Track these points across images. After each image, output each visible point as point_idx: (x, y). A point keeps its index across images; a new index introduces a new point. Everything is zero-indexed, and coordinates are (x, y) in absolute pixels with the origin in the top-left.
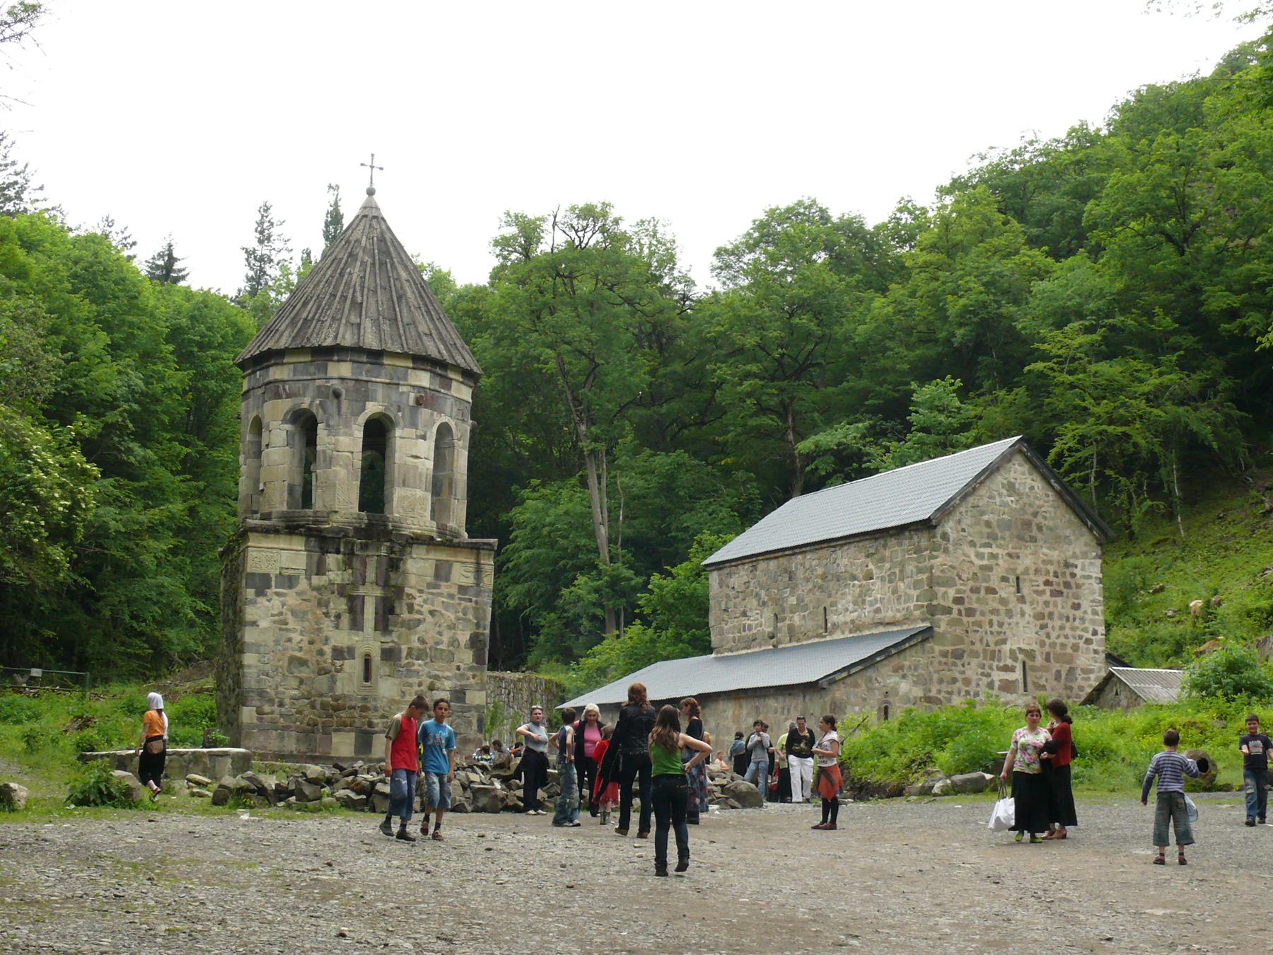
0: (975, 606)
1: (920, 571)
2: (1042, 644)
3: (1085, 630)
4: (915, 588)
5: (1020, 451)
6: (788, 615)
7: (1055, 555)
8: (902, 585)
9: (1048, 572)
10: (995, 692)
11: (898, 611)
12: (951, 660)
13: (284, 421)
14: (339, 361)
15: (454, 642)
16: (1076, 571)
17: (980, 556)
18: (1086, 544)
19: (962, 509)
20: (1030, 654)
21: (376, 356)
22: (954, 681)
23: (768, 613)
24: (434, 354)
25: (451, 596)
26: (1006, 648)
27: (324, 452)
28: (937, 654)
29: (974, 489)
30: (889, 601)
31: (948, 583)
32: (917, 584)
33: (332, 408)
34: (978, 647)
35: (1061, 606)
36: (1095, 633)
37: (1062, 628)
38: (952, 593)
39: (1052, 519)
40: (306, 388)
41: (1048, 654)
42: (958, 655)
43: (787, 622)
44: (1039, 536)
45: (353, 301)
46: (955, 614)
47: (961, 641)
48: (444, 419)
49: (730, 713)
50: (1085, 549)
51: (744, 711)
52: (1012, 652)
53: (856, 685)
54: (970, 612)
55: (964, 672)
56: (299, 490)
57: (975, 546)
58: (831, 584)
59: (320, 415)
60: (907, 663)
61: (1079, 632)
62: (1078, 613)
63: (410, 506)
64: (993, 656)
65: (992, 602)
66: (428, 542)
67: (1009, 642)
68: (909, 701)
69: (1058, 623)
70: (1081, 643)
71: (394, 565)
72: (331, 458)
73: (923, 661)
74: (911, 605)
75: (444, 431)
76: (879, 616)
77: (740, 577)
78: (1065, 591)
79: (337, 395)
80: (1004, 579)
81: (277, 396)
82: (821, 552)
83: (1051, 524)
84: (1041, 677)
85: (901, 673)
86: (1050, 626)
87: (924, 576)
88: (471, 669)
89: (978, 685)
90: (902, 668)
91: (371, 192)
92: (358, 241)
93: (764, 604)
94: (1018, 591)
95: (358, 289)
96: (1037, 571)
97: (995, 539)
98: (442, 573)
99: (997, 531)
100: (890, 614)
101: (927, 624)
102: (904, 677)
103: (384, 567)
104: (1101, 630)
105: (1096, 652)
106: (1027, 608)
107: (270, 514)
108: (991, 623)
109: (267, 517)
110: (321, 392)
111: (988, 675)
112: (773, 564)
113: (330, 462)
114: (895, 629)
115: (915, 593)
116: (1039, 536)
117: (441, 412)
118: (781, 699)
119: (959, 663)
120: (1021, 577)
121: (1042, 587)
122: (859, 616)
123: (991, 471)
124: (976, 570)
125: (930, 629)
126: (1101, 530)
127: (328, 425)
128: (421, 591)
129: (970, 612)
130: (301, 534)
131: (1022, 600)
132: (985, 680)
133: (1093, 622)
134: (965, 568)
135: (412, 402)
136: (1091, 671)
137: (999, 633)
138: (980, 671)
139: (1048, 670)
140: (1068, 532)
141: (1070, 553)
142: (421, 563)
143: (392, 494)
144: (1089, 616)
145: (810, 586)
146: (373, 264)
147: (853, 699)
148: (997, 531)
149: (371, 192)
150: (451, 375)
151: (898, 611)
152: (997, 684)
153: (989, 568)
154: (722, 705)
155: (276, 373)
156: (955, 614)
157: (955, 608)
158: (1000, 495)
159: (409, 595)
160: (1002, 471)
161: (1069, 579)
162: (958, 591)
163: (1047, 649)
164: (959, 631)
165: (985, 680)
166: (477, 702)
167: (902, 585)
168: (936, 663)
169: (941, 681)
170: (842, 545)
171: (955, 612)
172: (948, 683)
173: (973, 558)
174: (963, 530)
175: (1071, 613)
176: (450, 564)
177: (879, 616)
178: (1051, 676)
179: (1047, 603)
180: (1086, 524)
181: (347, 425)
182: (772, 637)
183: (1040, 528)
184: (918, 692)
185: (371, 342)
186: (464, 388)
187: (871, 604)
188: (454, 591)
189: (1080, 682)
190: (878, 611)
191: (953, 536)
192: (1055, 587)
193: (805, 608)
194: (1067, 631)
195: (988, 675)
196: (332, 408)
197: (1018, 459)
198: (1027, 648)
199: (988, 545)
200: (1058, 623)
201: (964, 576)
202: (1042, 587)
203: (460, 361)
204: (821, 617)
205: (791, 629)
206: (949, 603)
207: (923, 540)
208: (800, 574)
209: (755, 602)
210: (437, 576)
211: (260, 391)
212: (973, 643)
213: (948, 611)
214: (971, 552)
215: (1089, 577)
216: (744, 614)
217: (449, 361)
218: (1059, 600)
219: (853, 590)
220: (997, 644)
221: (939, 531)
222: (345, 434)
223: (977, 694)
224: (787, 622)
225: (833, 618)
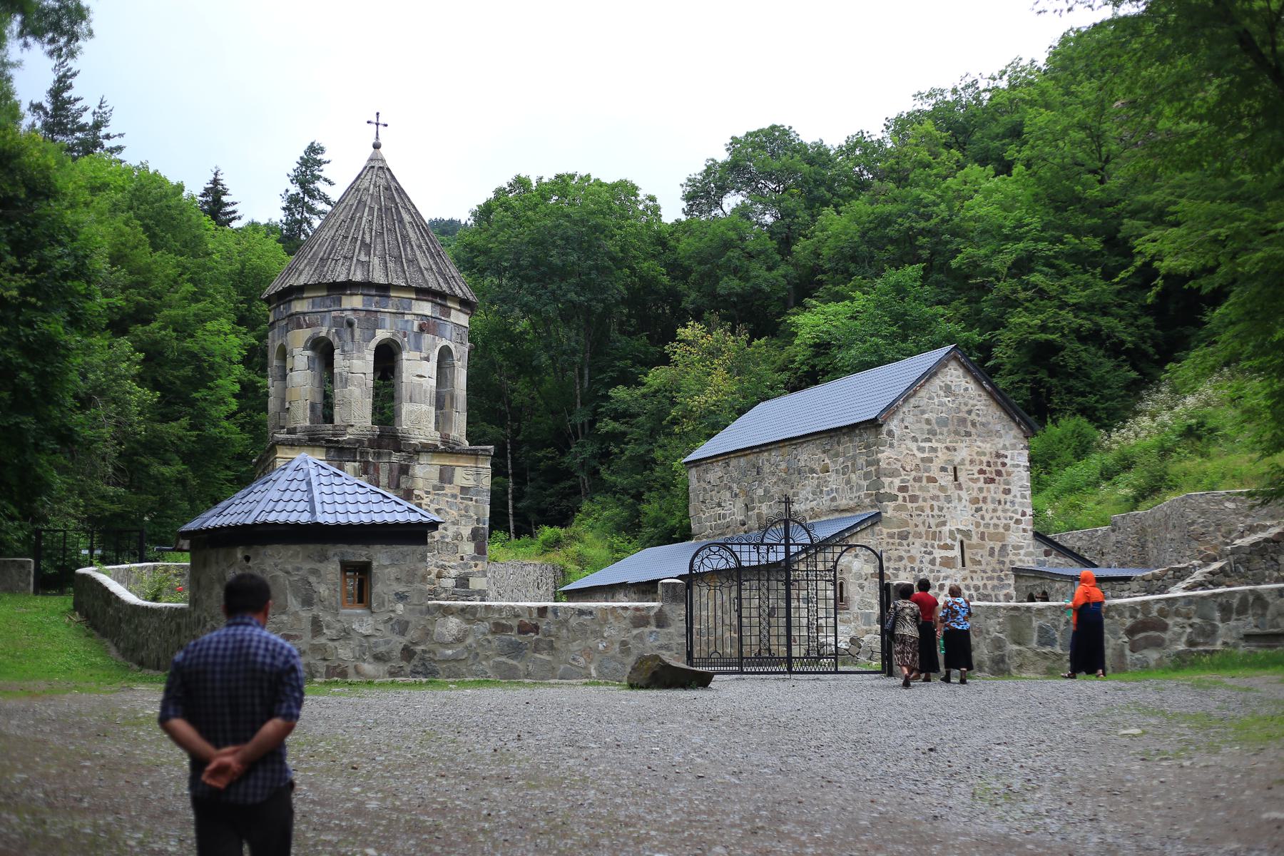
0: (918, 493)
1: (869, 464)
3: (1015, 512)
5: (955, 358)
7: (987, 447)
8: (853, 476)
9: (981, 463)
13: (305, 348)
14: (351, 295)
15: (458, 536)
17: (921, 449)
18: (1015, 437)
20: (967, 534)
21: (384, 289)
22: (901, 558)
23: (740, 503)
24: (433, 284)
25: (454, 496)
26: (946, 529)
27: (341, 374)
28: (885, 536)
29: (915, 392)
31: (893, 474)
32: (867, 476)
33: (347, 336)
34: (922, 529)
35: (994, 491)
36: (1024, 514)
37: (995, 510)
38: (897, 482)
40: (323, 319)
41: (983, 533)
42: (904, 536)
43: (756, 511)
44: (973, 431)
45: (363, 241)
46: (900, 501)
48: (445, 342)
50: (1014, 441)
52: (951, 532)
54: (914, 499)
56: (320, 407)
59: (336, 342)
61: (1010, 514)
62: (1009, 497)
63: (417, 420)
65: (933, 490)
66: (431, 450)
69: (991, 506)
70: (1012, 523)
71: (404, 470)
72: (347, 379)
74: (862, 494)
75: (445, 354)
77: (715, 473)
78: (997, 478)
79: (350, 324)
80: (943, 469)
81: (299, 326)
83: (984, 420)
88: (473, 558)
91: (377, 146)
92: (367, 189)
94: (956, 479)
95: (367, 231)
96: (972, 462)
98: (446, 476)
100: (844, 502)
102: (856, 556)
103: (395, 473)
104: (1029, 511)
105: (1024, 530)
106: (964, 494)
107: (295, 428)
108: (932, 508)
109: (292, 431)
110: (337, 322)
111: (931, 553)
113: (346, 382)
114: (848, 515)
115: (865, 483)
116: (973, 431)
117: (442, 336)
119: (905, 543)
121: (976, 476)
123: (930, 374)
124: (918, 462)
125: (879, 513)
126: (1027, 423)
127: (343, 351)
128: (428, 493)
129: (914, 499)
130: (321, 446)
132: (928, 557)
133: (1022, 504)
135: (416, 329)
136: (1021, 547)
137: (939, 516)
139: (982, 547)
140: (998, 427)
142: (428, 468)
143: (400, 409)
144: (1018, 500)
146: (380, 209)
149: (377, 146)
150: (449, 304)
152: (938, 561)
153: (931, 460)
155: (299, 306)
156: (900, 501)
157: (901, 495)
159: (417, 496)
160: (939, 375)
161: (1000, 468)
162: (902, 481)
163: (982, 529)
164: (904, 515)
165: (928, 557)
166: (478, 587)
167: (853, 476)
168: (884, 544)
171: (900, 499)
173: (916, 452)
174: (906, 427)
175: (1002, 497)
176: (453, 468)
179: (981, 490)
180: (1014, 420)
181: (360, 350)
183: (974, 424)
185: (378, 277)
186: (461, 315)
188: (457, 491)
189: (1011, 557)
190: (833, 499)
191: (897, 432)
194: (999, 513)
195: (931, 553)
196: (347, 336)
197: (953, 365)
198: (961, 527)
200: (991, 506)
201: (908, 468)
202: (976, 476)
203: (458, 292)
207: (869, 437)
208: (767, 468)
209: (728, 494)
210: (442, 479)
211: (284, 322)
212: (916, 526)
213: (895, 498)
214: (914, 446)
215: (1018, 466)
216: (719, 505)
217: (448, 292)
218: (992, 486)
219: (811, 482)
220: (937, 526)
221: (885, 429)
222: (359, 358)
224: (756, 511)
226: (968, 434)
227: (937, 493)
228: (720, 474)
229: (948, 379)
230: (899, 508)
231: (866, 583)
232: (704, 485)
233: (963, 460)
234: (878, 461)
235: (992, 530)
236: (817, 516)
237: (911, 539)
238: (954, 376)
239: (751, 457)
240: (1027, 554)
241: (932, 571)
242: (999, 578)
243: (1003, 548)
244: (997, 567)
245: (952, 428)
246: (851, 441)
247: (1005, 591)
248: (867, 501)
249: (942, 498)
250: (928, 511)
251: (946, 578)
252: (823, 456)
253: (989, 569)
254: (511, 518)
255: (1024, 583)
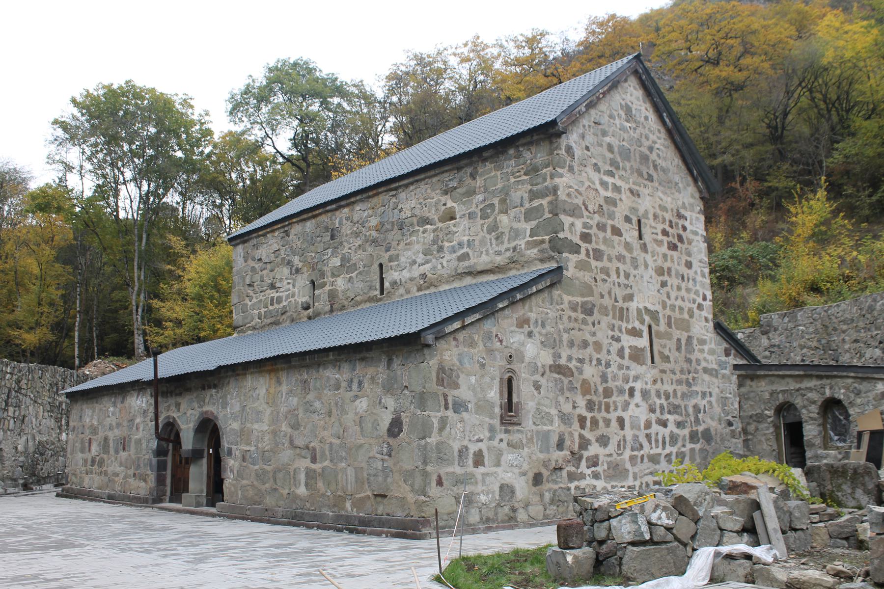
0: (602, 247)
1: (533, 195)
2: (664, 306)
4: (527, 219)
5: (636, 72)
6: (329, 279)
8: (504, 219)
9: (664, 221)
10: (626, 362)
11: (498, 253)
12: (582, 316)
16: (687, 224)
17: (604, 184)
18: (692, 196)
19: (585, 121)
20: (654, 315)
22: (585, 344)
23: (303, 281)
26: (633, 305)
28: (566, 306)
30: (483, 242)
31: (574, 212)
32: (529, 215)
34: (607, 302)
36: (705, 299)
39: (665, 159)
41: (669, 317)
42: (588, 310)
43: (328, 288)
46: (583, 256)
47: (591, 294)
49: (262, 391)
50: (692, 201)
51: (284, 388)
52: (639, 311)
53: (472, 344)
54: (598, 255)
55: (594, 334)
57: (599, 171)
58: (390, 236)
60: (533, 316)
61: (692, 296)
62: (691, 272)
64: (622, 314)
67: (635, 299)
68: (535, 370)
73: (552, 314)
74: (522, 243)
76: (466, 264)
78: (679, 244)
80: (628, 219)
82: (375, 200)
83: (664, 164)
84: (665, 346)
85: (526, 329)
86: (669, 284)
87: (545, 202)
89: (609, 352)
90: (527, 321)
93: (298, 271)
94: (640, 237)
96: (655, 216)
97: (618, 168)
99: (619, 160)
100: (484, 258)
101: (554, 265)
102: (530, 334)
104: (709, 296)
105: (706, 320)
106: (648, 257)
111: (618, 340)
112: (310, 225)
114: (491, 277)
115: (528, 227)
118: (346, 367)
119: (590, 319)
120: (643, 221)
121: (660, 237)
122: (434, 268)
123: (613, 84)
125: (560, 269)
126: (704, 182)
129: (598, 255)
131: (644, 248)
132: (616, 346)
133: (703, 285)
134: (591, 196)
137: (626, 286)
138: (610, 333)
139: (669, 336)
140: (677, 178)
141: (680, 203)
144: (699, 278)
145: (359, 242)
147: (467, 365)
148: (619, 160)
151: (498, 253)
152: (627, 351)
154: (250, 381)
156: (583, 256)
157: (584, 246)
158: (619, 116)
161: (681, 232)
162: (585, 226)
163: (668, 312)
164: (587, 277)
165: (616, 346)
168: (565, 318)
169: (571, 344)
170: (406, 186)
171: (583, 251)
172: (579, 347)
173: (598, 187)
175: (683, 270)
177: (466, 264)
178: (672, 344)
179: (665, 256)
182: (307, 308)
183: (655, 167)
184: (546, 358)
187: (453, 250)
190: (465, 257)
191: (578, 152)
192: (670, 239)
193: (354, 267)
194: (683, 293)
195: (618, 340)
197: (633, 82)
198: (651, 308)
199: (611, 174)
200: (673, 281)
204: (377, 277)
205: (332, 295)
206: (576, 239)
207: (537, 155)
209: (286, 271)
212: (602, 296)
214: (595, 176)
215: (695, 233)
216: (273, 286)
218: (674, 253)
219: (424, 237)
221: (563, 141)
223: (608, 365)
224: (328, 288)
225: (391, 276)
226: (650, 178)
227: (625, 253)
228: (275, 247)
229: (628, 98)
230: (582, 266)
231: (543, 381)
232: (251, 263)
233: (646, 212)
234: (555, 189)
235: (677, 314)
236: (432, 285)
237: (596, 315)
238: (632, 94)
239: (323, 218)
240: (712, 352)
241: (621, 367)
242: (689, 385)
243: (689, 338)
244: (686, 366)
245: (636, 166)
246: (498, 168)
247: (693, 402)
248: (533, 252)
249: (628, 260)
250: (614, 276)
251: (636, 378)
252: (443, 199)
253: (678, 369)
254: (76, 345)
255: (763, 388)
